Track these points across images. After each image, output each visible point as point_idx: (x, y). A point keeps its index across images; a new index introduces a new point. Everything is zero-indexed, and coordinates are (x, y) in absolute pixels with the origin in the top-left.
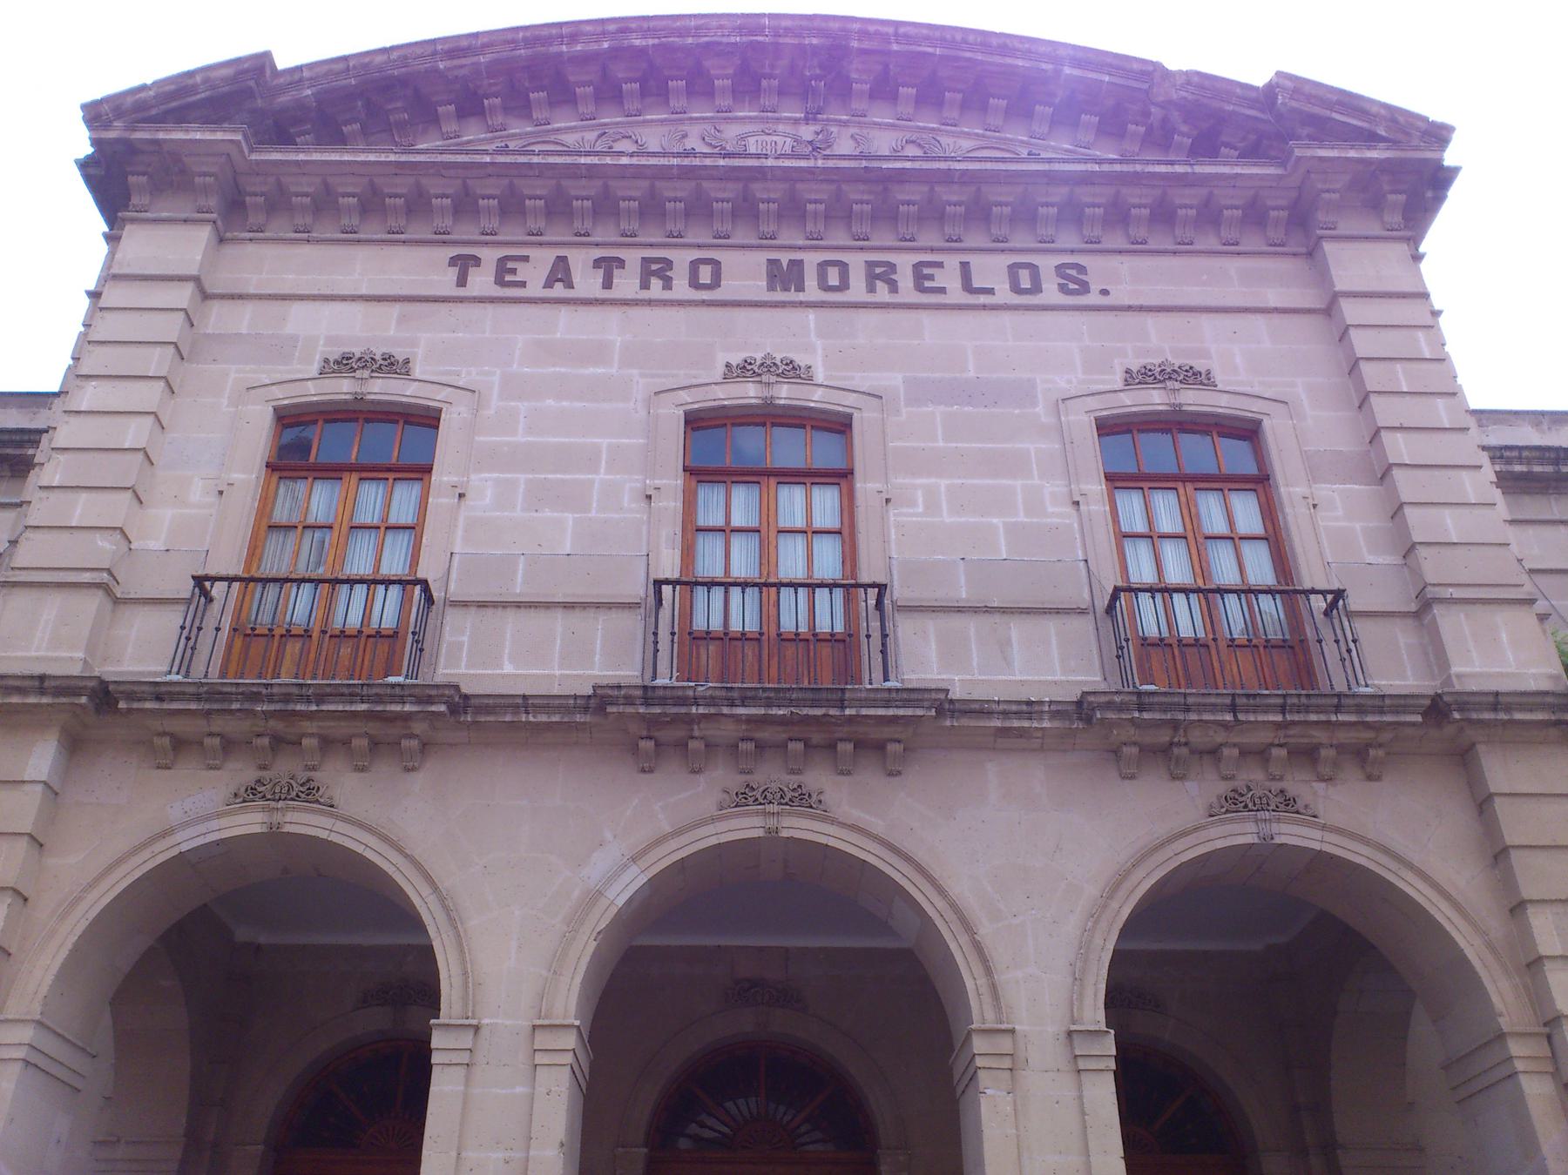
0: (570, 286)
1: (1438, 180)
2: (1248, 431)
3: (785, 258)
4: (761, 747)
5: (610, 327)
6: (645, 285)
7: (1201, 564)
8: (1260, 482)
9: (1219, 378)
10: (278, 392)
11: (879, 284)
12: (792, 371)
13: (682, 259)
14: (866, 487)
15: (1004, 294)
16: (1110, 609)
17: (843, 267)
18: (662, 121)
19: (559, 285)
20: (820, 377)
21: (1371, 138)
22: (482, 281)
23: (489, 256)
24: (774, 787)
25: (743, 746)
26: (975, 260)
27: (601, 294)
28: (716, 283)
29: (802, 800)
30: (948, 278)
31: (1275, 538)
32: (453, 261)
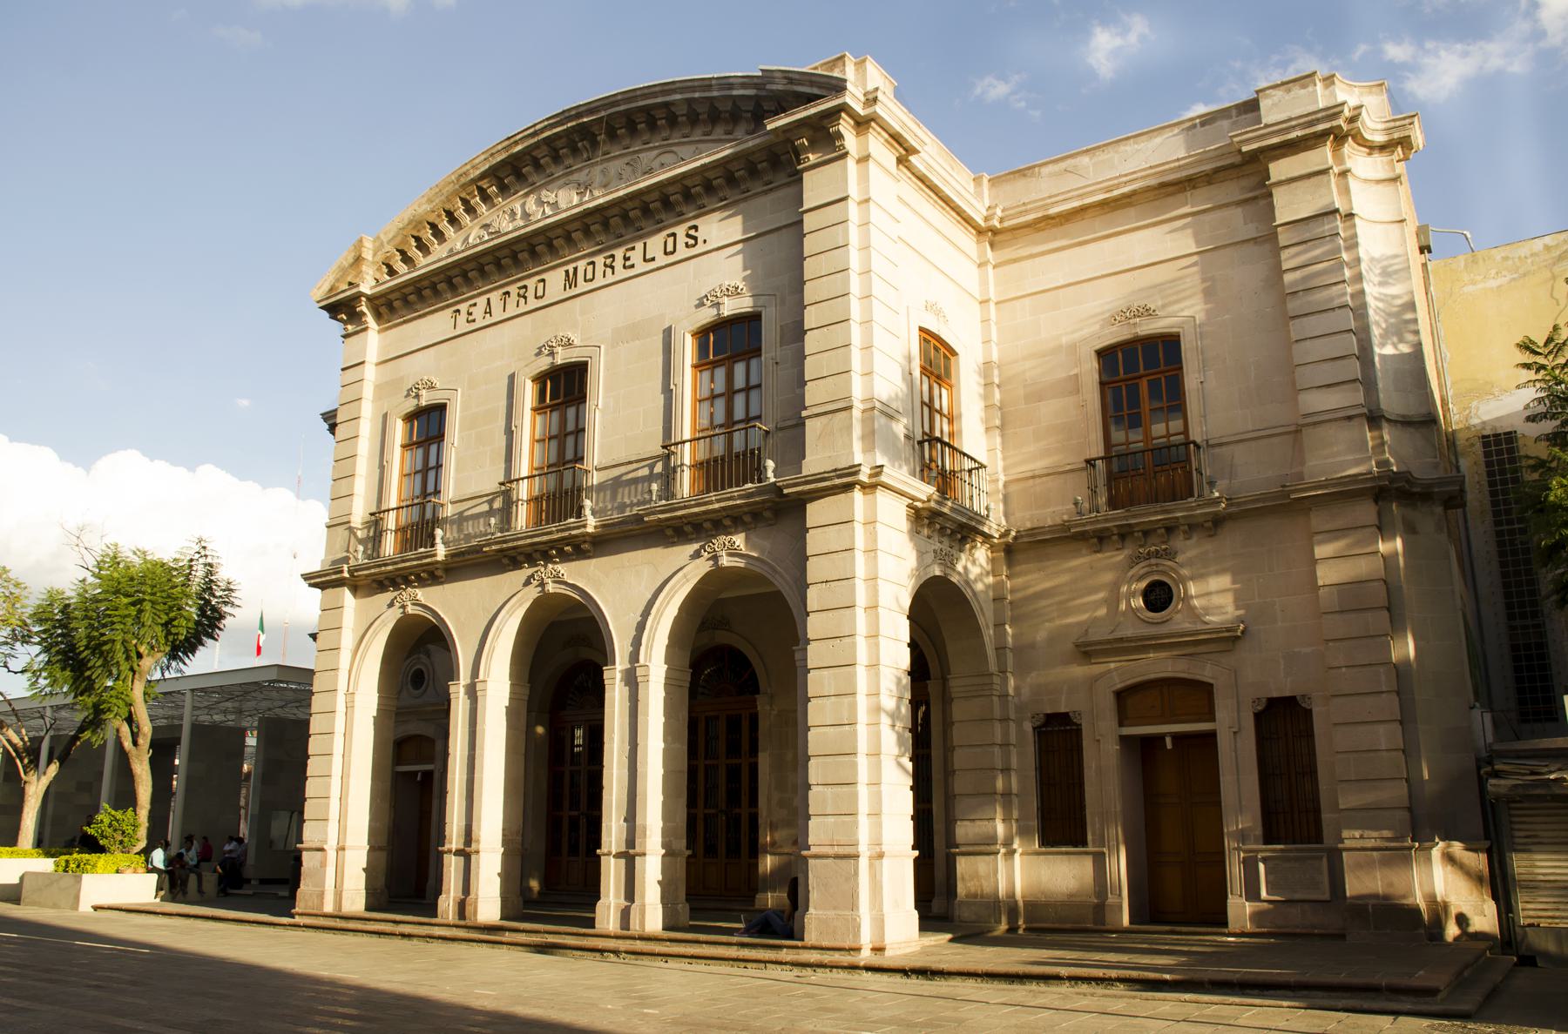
21: (811, 99)
22: (462, 318)
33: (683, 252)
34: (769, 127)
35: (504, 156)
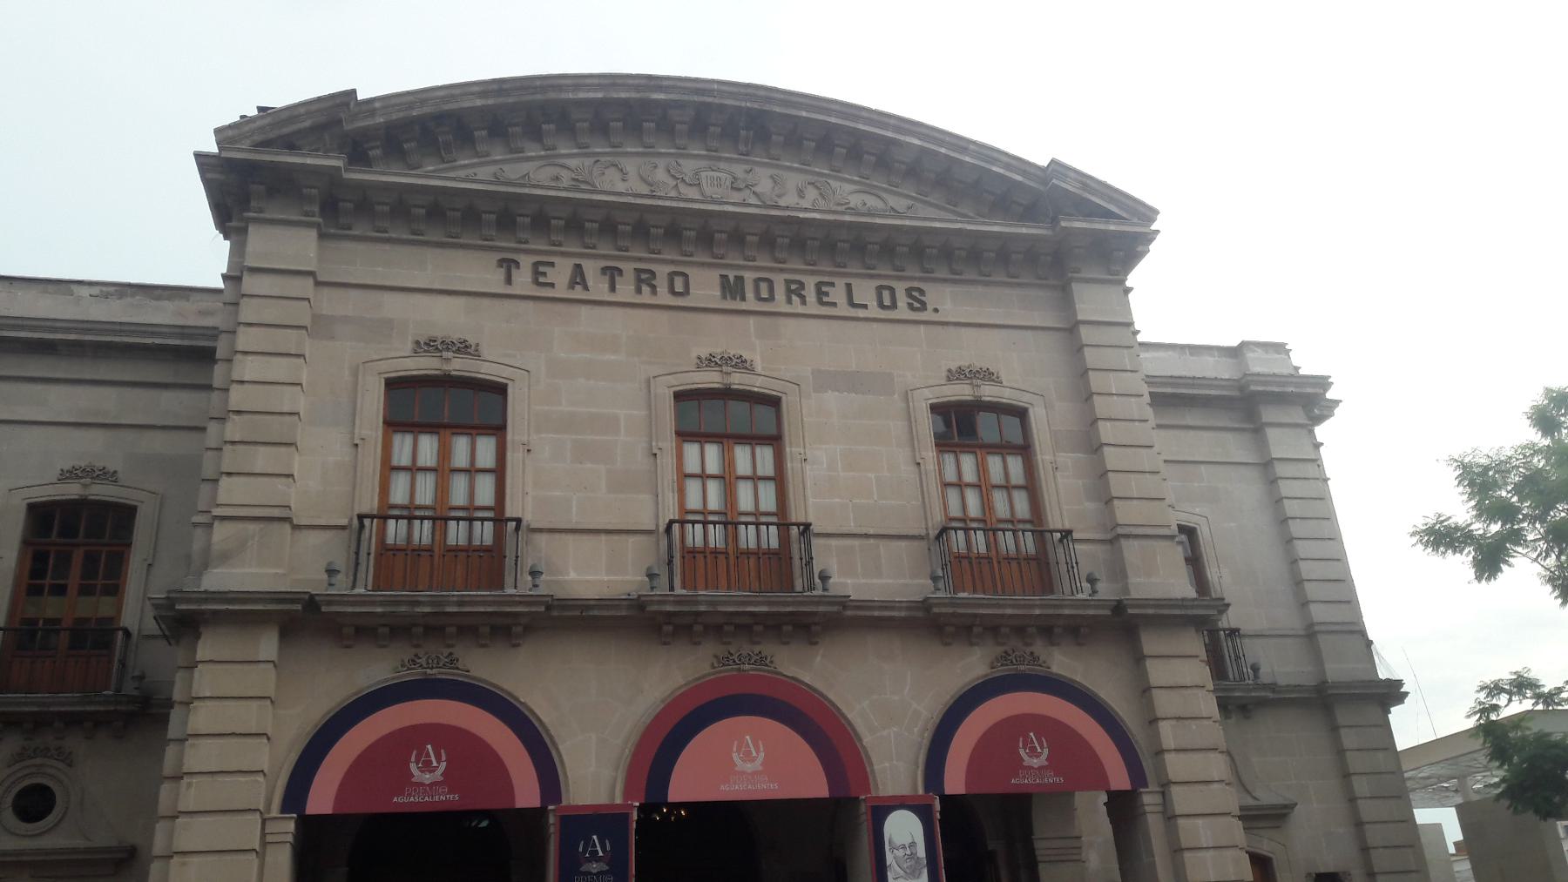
0: (586, 288)
1: (1149, 237)
2: (1021, 413)
3: (731, 275)
4: (738, 627)
5: (617, 323)
6: (639, 291)
7: (987, 505)
8: (1025, 450)
9: (1003, 378)
10: (384, 366)
11: (794, 298)
12: (742, 364)
13: (662, 271)
14: (790, 450)
15: (874, 311)
16: (938, 537)
17: (770, 282)
18: (637, 154)
19: (578, 287)
20: (759, 369)
21: (1108, 215)
22: (523, 280)
23: (526, 262)
24: (744, 653)
25: (726, 628)
26: (854, 282)
28: (686, 292)
30: (837, 294)
31: (1032, 487)
32: (501, 262)
33: (903, 312)
34: (1063, 224)
35: (634, 95)
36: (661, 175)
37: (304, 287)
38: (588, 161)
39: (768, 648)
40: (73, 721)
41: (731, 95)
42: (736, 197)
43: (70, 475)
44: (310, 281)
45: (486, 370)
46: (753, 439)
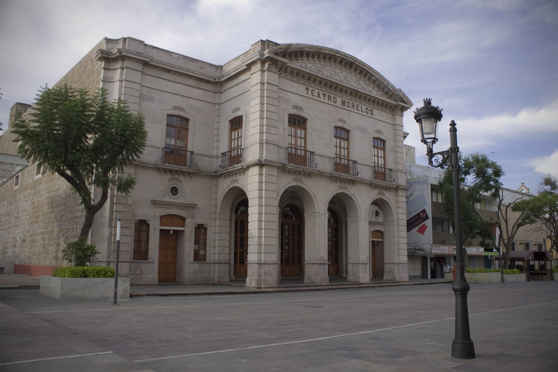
3: (343, 99)
8: (384, 150)
14: (351, 143)
21: (405, 103)
22: (310, 92)
27: (323, 101)
29: (346, 188)
36: (333, 73)
37: (276, 89)
38: (321, 66)
39: (347, 185)
40: (183, 173)
41: (350, 58)
42: (345, 81)
43: (175, 108)
44: (277, 88)
45: (305, 116)
46: (344, 139)
